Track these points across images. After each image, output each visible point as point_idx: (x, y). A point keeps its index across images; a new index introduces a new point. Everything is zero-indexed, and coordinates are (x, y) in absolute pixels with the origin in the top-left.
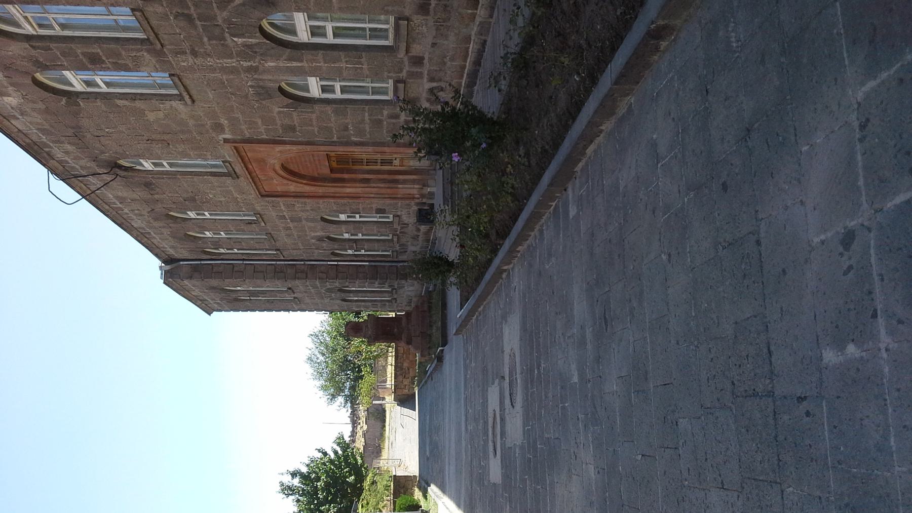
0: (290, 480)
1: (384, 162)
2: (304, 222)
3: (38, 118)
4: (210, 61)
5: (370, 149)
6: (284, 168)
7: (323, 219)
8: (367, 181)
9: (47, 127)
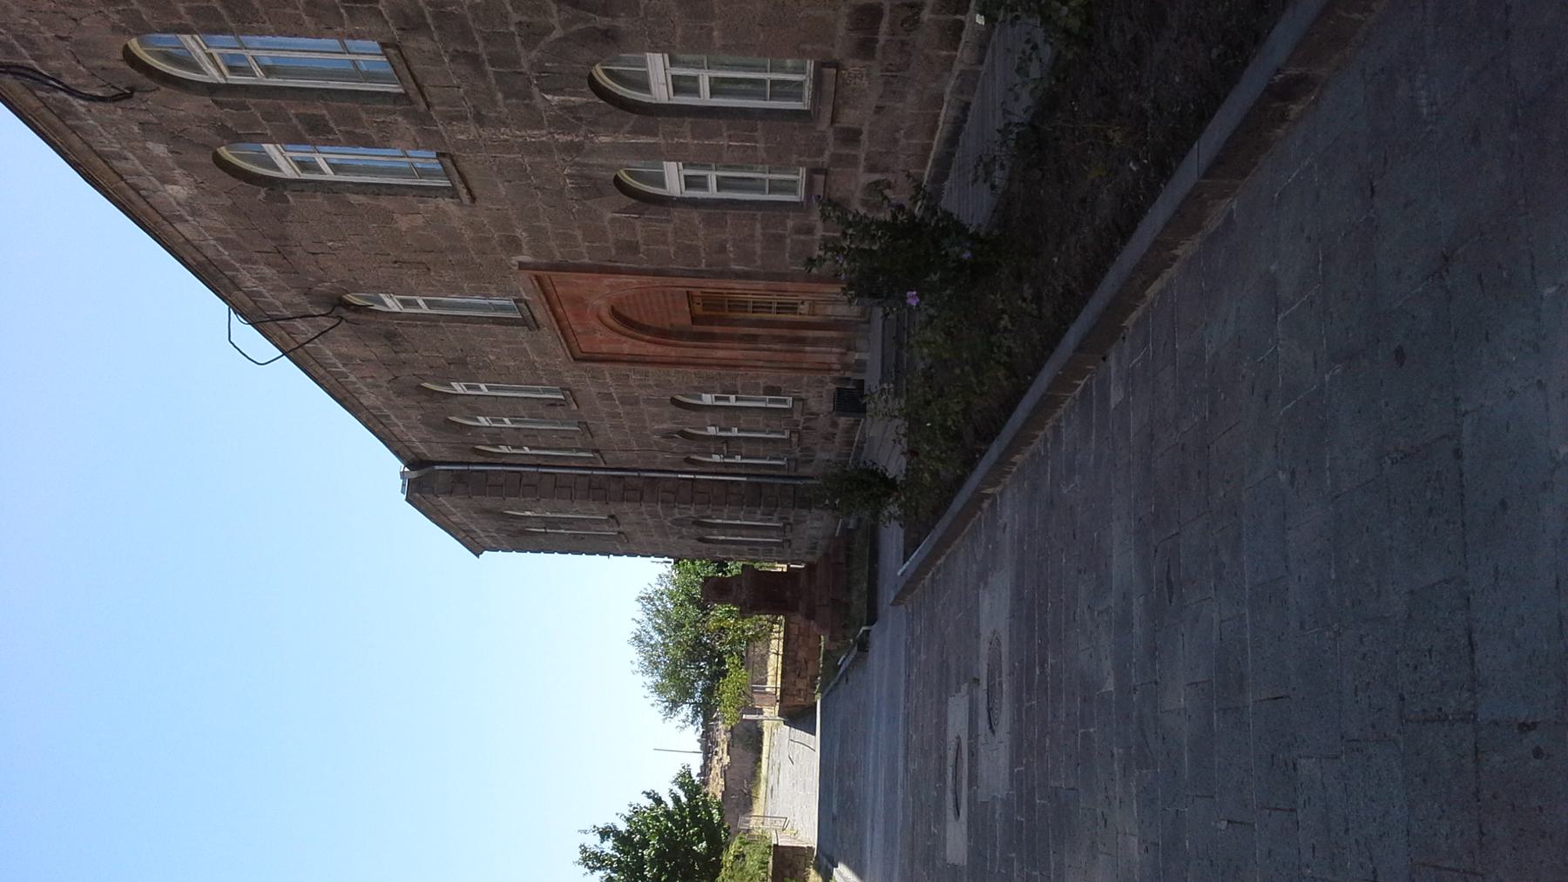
0: (598, 843)
1: (782, 308)
2: (642, 406)
3: (218, 221)
4: (505, 134)
5: (761, 284)
6: (615, 313)
7: (674, 402)
8: (753, 338)
9: (232, 236)
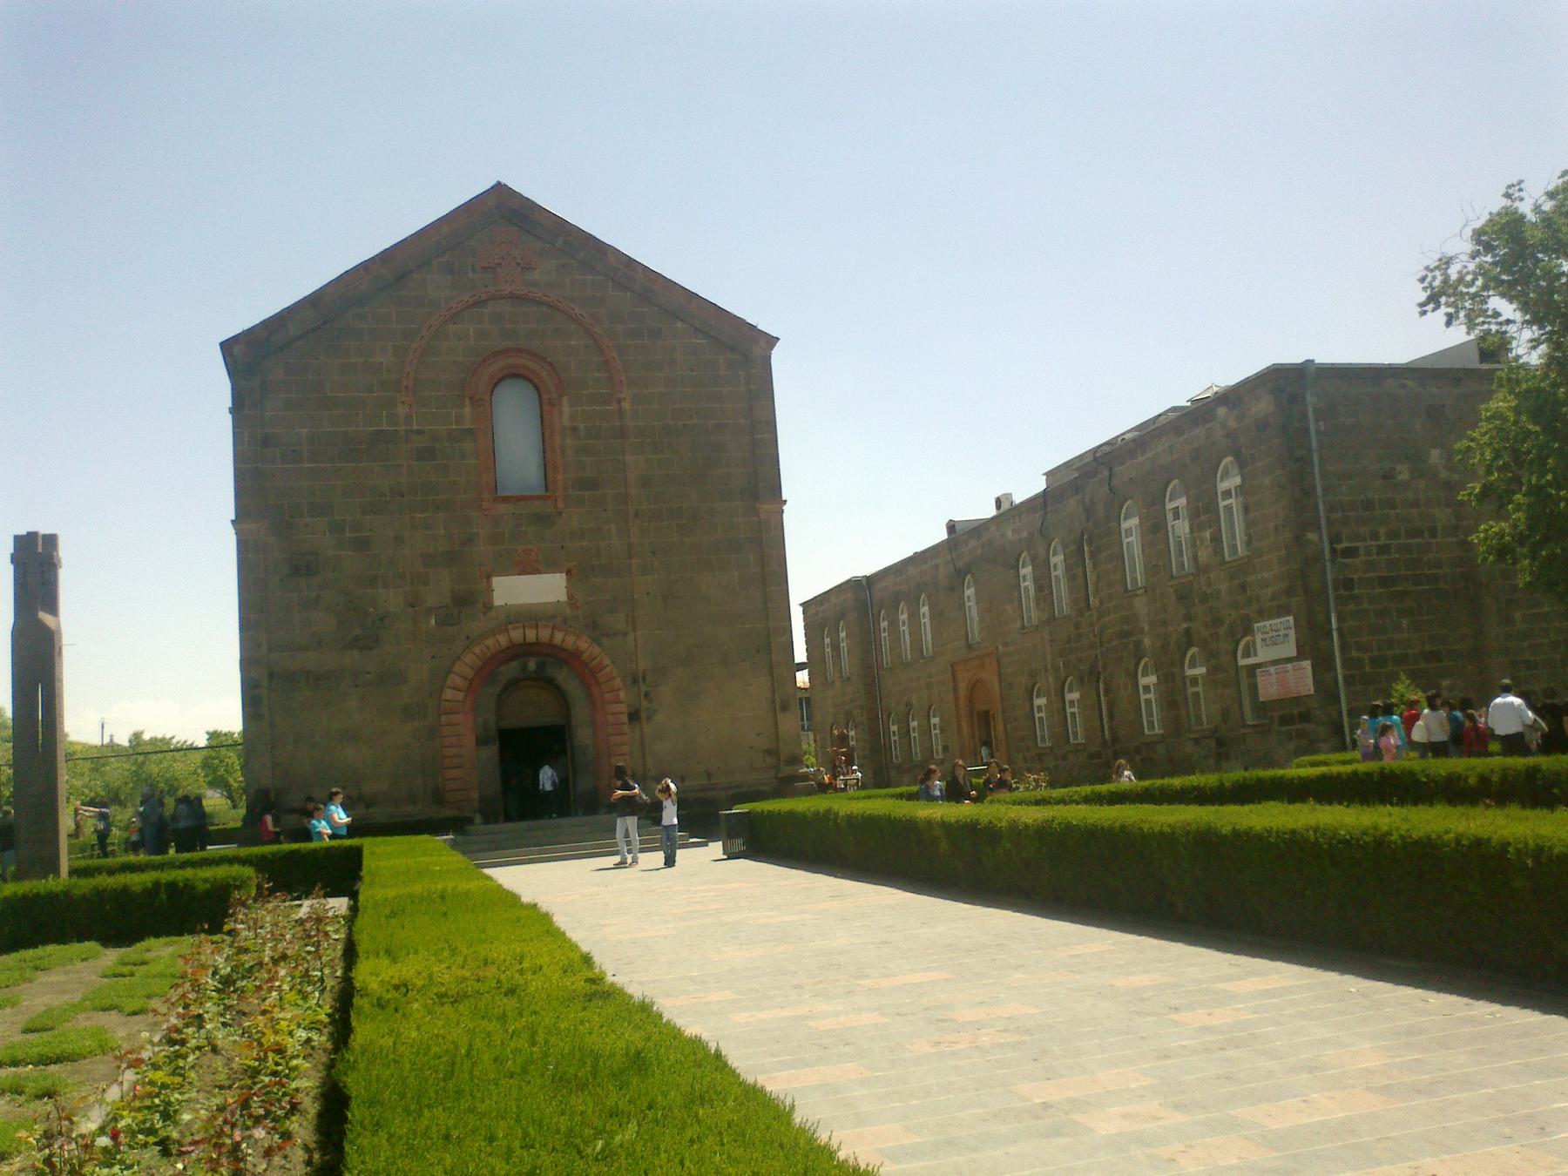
6: (977, 680)
